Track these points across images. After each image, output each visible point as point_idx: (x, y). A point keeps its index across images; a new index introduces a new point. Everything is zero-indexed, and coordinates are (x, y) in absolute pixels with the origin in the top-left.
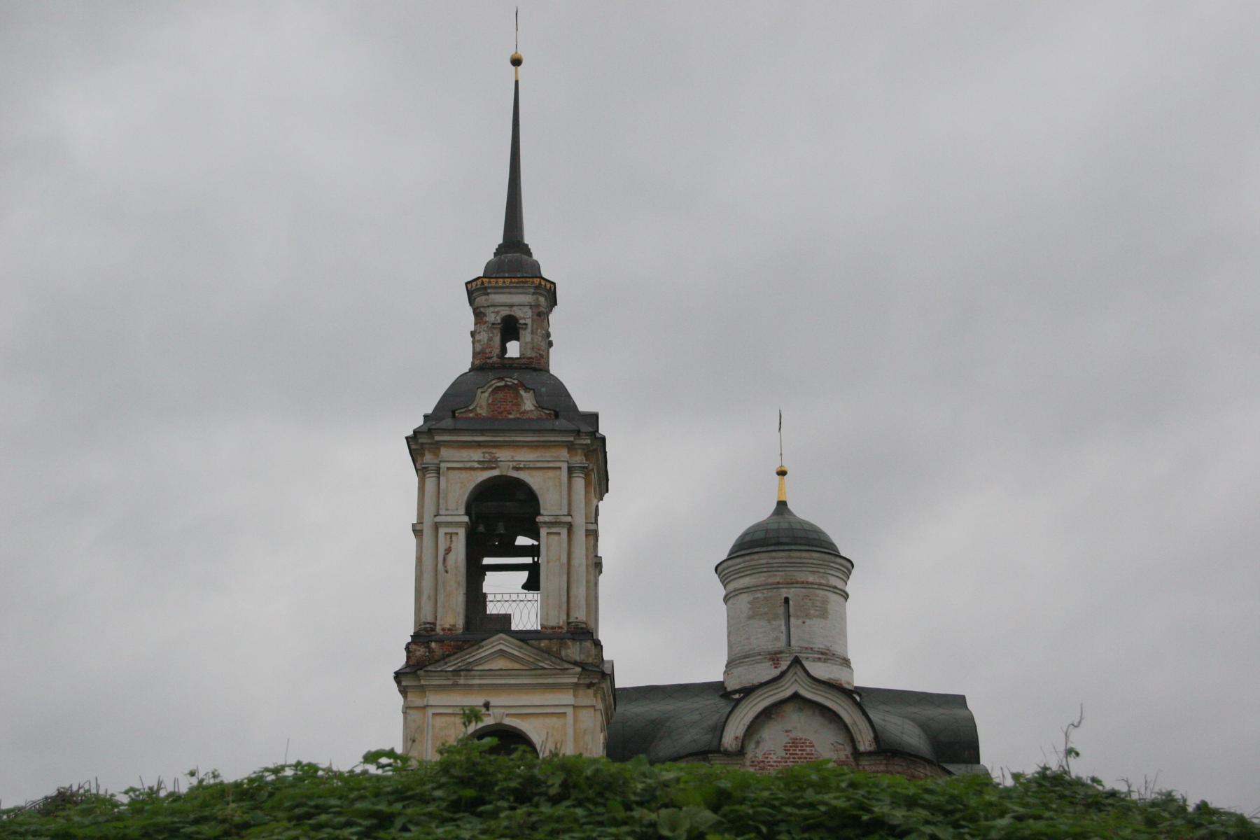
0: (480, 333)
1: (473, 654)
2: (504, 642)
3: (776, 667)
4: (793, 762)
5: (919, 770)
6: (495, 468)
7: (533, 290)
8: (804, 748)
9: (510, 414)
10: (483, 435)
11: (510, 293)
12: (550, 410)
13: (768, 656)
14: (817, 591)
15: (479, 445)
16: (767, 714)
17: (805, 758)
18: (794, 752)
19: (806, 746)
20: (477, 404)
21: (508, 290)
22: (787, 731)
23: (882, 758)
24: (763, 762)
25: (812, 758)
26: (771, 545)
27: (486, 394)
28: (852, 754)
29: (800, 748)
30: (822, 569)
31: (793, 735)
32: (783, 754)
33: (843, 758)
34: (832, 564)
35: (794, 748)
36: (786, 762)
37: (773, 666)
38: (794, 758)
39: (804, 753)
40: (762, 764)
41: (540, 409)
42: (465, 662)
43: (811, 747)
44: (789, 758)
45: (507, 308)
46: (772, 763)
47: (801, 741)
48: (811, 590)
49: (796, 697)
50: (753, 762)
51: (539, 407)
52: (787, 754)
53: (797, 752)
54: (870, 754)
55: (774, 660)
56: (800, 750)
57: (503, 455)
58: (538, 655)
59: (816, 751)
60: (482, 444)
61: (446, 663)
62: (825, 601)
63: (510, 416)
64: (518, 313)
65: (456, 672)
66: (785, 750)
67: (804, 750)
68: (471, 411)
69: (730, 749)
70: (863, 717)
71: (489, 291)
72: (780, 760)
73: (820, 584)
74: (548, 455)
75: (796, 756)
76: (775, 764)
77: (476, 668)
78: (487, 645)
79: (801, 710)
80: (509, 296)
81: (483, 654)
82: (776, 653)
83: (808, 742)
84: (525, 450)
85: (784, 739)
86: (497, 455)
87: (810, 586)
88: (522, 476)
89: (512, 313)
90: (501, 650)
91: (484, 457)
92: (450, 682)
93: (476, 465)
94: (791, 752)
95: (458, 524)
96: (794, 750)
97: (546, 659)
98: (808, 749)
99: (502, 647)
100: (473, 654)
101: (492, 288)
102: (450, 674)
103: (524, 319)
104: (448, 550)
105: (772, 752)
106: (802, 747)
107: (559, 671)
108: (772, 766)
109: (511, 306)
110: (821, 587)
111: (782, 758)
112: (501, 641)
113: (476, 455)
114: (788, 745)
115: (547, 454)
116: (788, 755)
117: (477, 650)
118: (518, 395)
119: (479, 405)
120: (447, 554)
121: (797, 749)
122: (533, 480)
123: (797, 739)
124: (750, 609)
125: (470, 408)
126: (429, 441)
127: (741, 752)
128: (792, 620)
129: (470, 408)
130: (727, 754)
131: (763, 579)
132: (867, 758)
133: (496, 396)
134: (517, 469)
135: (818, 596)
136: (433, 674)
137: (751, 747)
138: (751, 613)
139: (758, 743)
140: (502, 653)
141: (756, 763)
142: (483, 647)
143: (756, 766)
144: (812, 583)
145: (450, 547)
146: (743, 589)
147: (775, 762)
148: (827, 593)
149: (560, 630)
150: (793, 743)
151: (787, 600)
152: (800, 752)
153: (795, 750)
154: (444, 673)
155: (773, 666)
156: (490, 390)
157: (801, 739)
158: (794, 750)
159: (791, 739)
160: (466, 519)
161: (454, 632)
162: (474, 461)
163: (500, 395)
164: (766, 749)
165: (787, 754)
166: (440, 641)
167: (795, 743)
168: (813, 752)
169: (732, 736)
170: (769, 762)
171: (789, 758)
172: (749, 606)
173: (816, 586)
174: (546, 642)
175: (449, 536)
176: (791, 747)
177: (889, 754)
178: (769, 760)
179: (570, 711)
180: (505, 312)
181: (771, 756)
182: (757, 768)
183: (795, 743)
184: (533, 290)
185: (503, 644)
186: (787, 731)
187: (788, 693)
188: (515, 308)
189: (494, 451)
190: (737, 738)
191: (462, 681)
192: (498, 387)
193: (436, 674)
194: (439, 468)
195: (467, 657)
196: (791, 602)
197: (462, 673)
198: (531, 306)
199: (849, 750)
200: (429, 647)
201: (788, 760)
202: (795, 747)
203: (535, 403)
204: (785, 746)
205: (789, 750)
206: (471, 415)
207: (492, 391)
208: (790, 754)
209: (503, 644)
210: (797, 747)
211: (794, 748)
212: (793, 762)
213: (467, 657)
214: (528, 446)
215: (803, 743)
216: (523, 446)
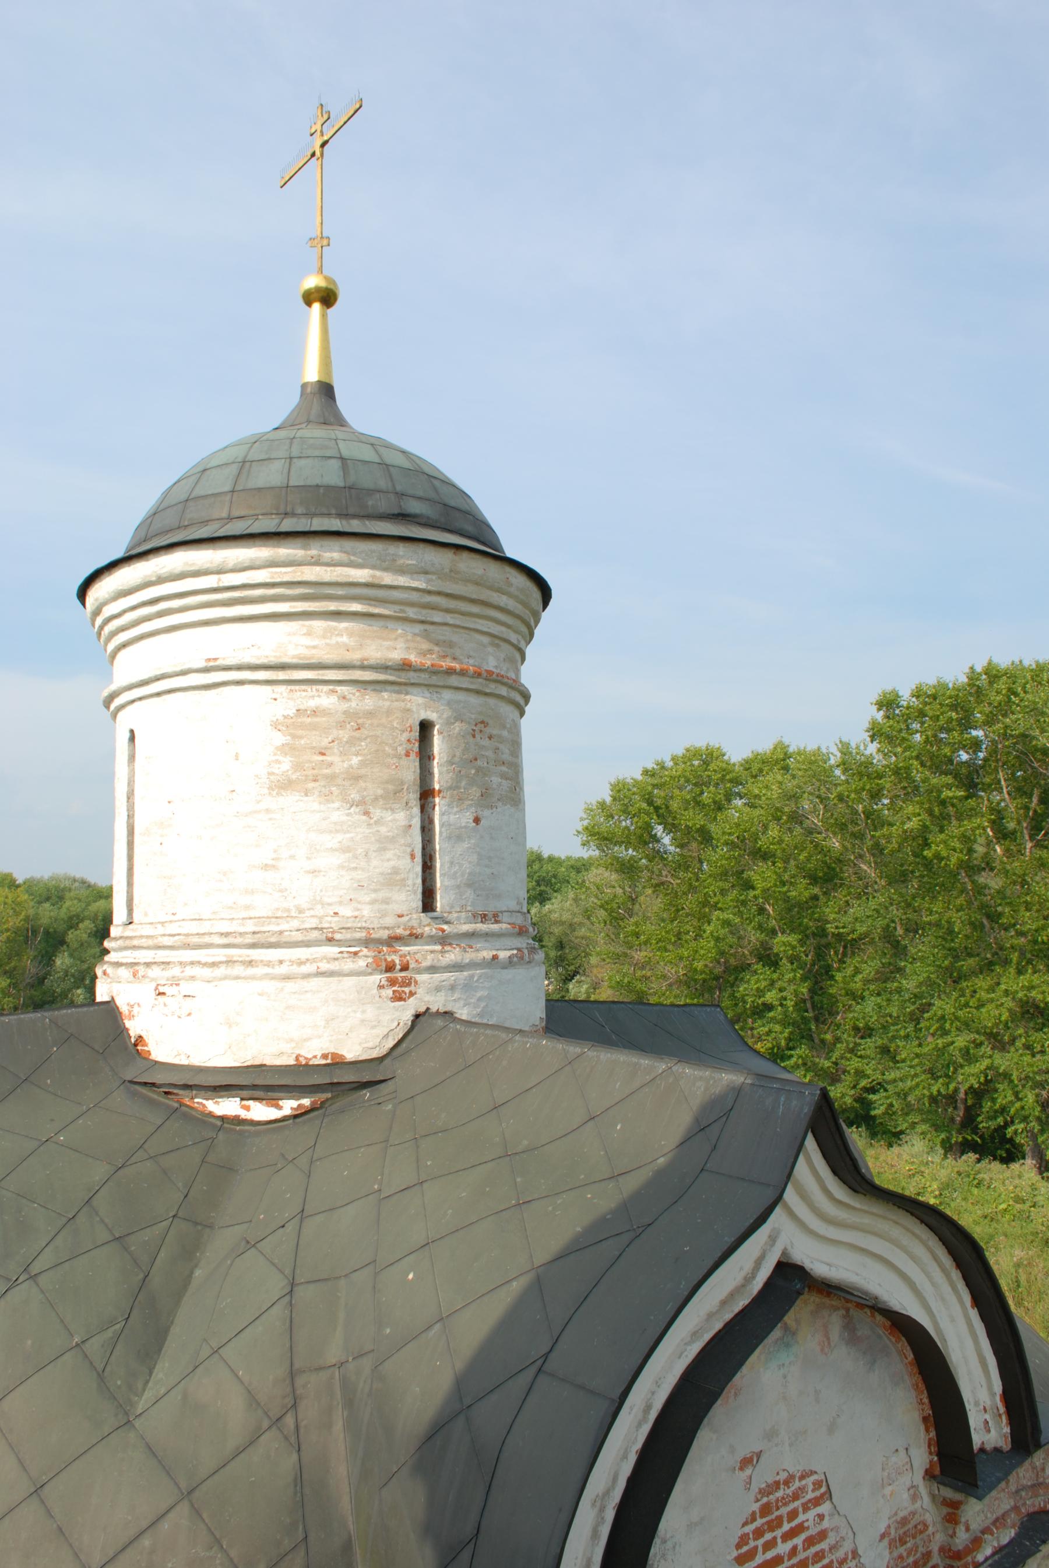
3: (398, 998)
31: (763, 1475)
37: (389, 992)
48: (492, 701)
55: (390, 968)
82: (394, 940)
83: (809, 1481)
124: (285, 749)
131: (345, 639)
135: (504, 727)
138: (286, 764)
146: (239, 668)
150: (765, 1510)
151: (425, 728)
168: (826, 1524)
172: (280, 739)
196: (438, 744)
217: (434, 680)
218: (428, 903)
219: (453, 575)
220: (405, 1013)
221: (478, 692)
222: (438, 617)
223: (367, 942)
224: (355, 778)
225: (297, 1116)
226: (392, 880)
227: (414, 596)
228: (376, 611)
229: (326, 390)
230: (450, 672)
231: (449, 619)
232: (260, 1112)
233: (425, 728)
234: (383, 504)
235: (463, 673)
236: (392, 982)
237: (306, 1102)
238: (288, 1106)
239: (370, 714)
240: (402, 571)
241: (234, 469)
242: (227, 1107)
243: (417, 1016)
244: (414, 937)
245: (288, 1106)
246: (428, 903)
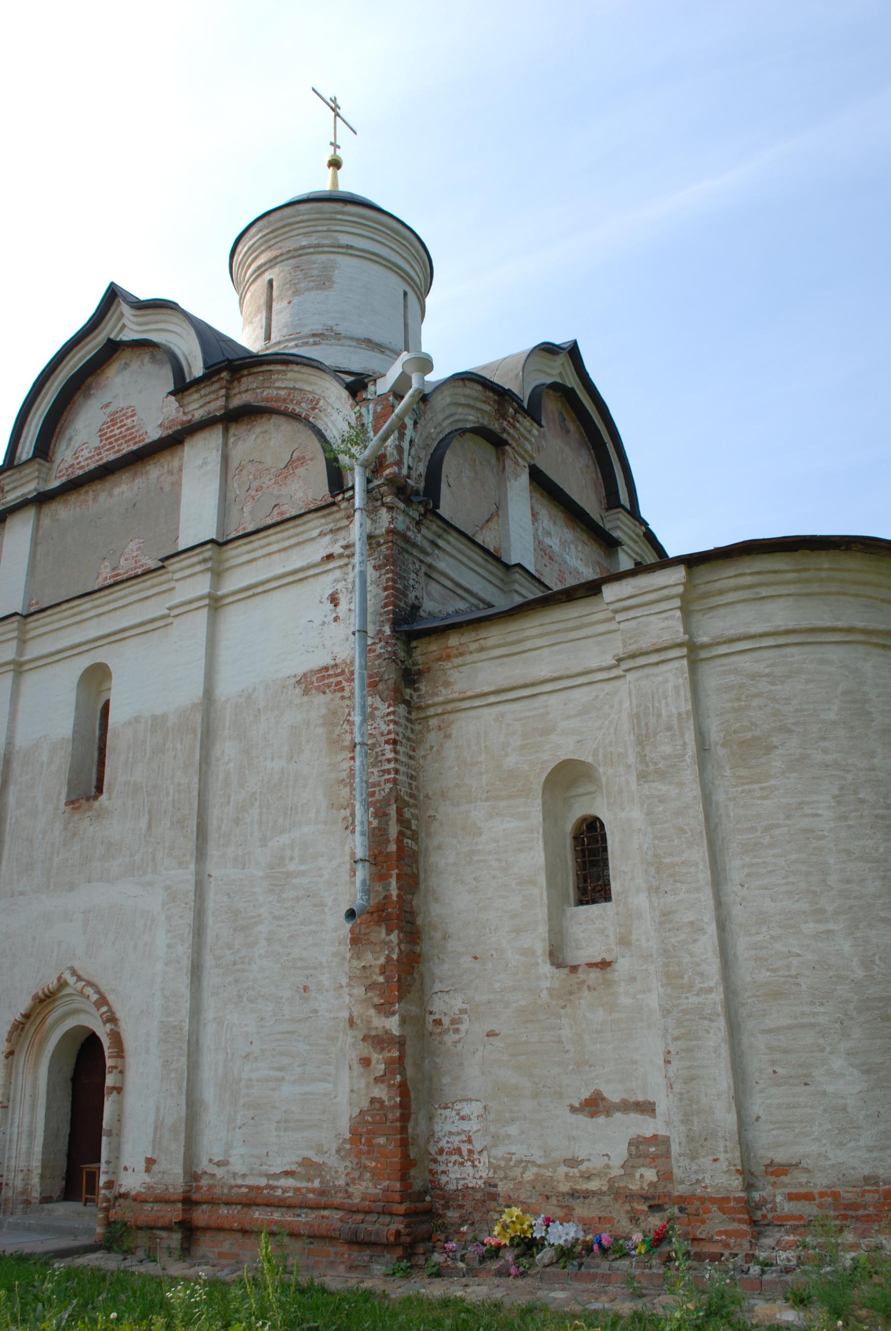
5: (278, 384)
14: (314, 257)
30: (323, 225)
34: (339, 217)
38: (110, 443)
44: (103, 446)
48: (304, 258)
52: (101, 441)
87: (301, 252)
96: (111, 431)
148: (332, 257)
150: (112, 420)
168: (135, 423)
196: (275, 284)
217: (272, 263)
221: (294, 257)
222: (272, 242)
227: (261, 241)
230: (276, 258)
231: (277, 240)
235: (281, 255)
240: (254, 236)
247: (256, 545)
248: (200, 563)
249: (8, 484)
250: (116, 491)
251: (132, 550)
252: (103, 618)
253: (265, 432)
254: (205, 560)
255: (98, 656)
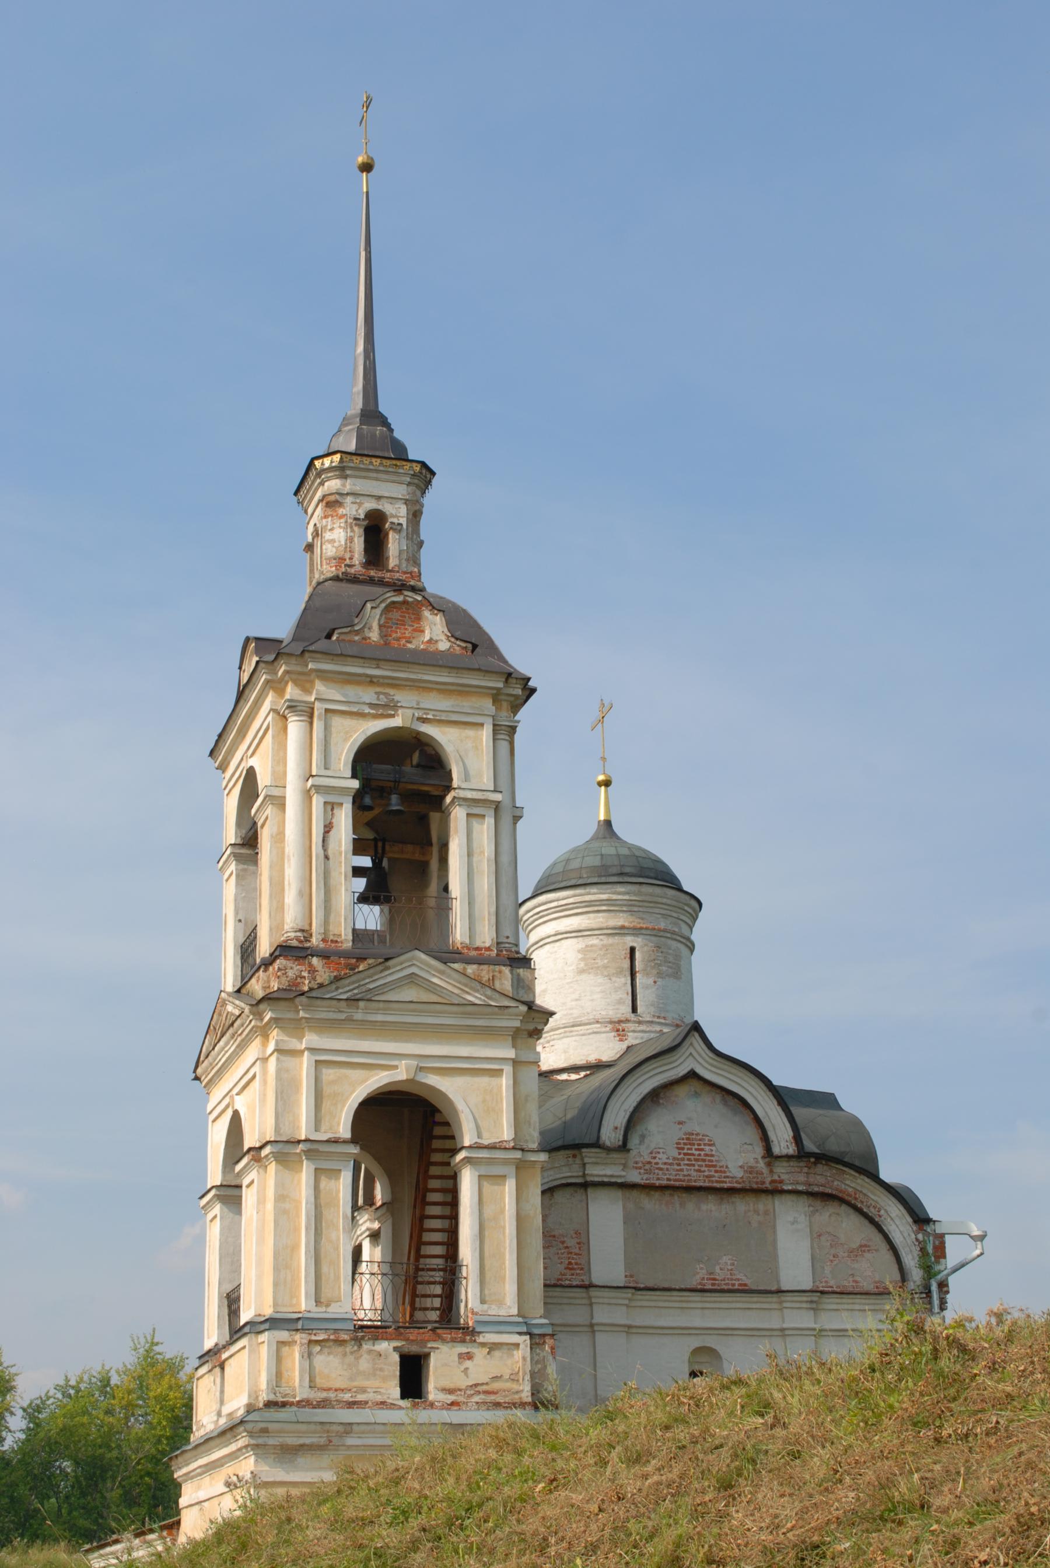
0: (332, 530)
1: (376, 977)
2: (418, 964)
3: (621, 1040)
4: (687, 1165)
5: (847, 1182)
6: (393, 716)
7: (408, 479)
8: (702, 1147)
9: (410, 642)
10: (378, 667)
11: (377, 479)
12: (466, 642)
13: (610, 1026)
14: (670, 942)
15: (371, 681)
16: (654, 1096)
17: (704, 1160)
18: (689, 1152)
19: (705, 1145)
20: (366, 624)
21: (375, 475)
22: (680, 1123)
23: (802, 1164)
24: (649, 1163)
25: (712, 1161)
26: (614, 875)
27: (378, 611)
28: (763, 1157)
29: (696, 1147)
30: (676, 912)
31: (687, 1128)
32: (675, 1153)
33: (752, 1163)
35: (689, 1146)
36: (679, 1165)
37: (618, 1038)
38: (689, 1160)
39: (702, 1153)
40: (647, 1167)
41: (453, 640)
42: (364, 989)
43: (710, 1145)
44: (683, 1159)
45: (373, 500)
46: (661, 1166)
47: (698, 1138)
48: (663, 939)
49: (692, 1075)
50: (636, 1163)
51: (452, 636)
52: (680, 1154)
53: (694, 1152)
54: (788, 1157)
55: (618, 1030)
56: (696, 1150)
57: (403, 697)
58: (466, 985)
59: (717, 1151)
60: (375, 680)
61: (337, 989)
62: (678, 957)
63: (409, 646)
64: (387, 508)
65: (353, 1001)
66: (678, 1148)
67: (702, 1150)
68: (357, 632)
69: (608, 1143)
70: (779, 1109)
71: (348, 472)
72: (671, 1161)
73: (674, 933)
74: (467, 704)
75: (692, 1157)
76: (665, 1167)
77: (376, 998)
78: (395, 966)
79: (697, 1094)
80: (375, 483)
81: (389, 979)
82: (620, 1022)
84: (433, 694)
85: (676, 1134)
86: (396, 698)
87: (662, 934)
88: (425, 729)
89: (380, 507)
90: (413, 973)
91: (378, 699)
92: (343, 1016)
93: (367, 710)
94: (685, 1151)
95: (342, 791)
96: (688, 1149)
97: (477, 991)
98: (707, 1148)
99: (413, 970)
100: (376, 977)
101: (351, 468)
102: (343, 1004)
103: (397, 517)
104: (328, 828)
105: (661, 1151)
106: (699, 1145)
107: (497, 1009)
108: (661, 1169)
109: (379, 498)
110: (675, 937)
111: (674, 1159)
112: (415, 962)
113: (368, 695)
114: (682, 1141)
115: (465, 704)
116: (682, 1156)
117: (382, 971)
118: (419, 618)
119: (367, 626)
120: (328, 832)
121: (694, 1147)
122: (445, 738)
123: (693, 1134)
124: (582, 959)
125: (357, 628)
126: (299, 669)
127: (624, 1147)
128: (639, 977)
129: (357, 628)
130: (609, 1150)
131: (601, 920)
132: (785, 1164)
133: (390, 615)
134: (424, 720)
135: (670, 949)
136: (319, 1002)
137: (634, 1142)
138: (582, 965)
139: (643, 1137)
140: (412, 979)
141: (640, 1165)
142: (388, 968)
143: (640, 1168)
144: (665, 931)
145: (331, 823)
146: (566, 933)
147: (665, 1164)
148: (679, 945)
149: (488, 953)
150: (688, 1139)
151: (632, 950)
152: (697, 1153)
153: (691, 1149)
154: (334, 1002)
155: (618, 1038)
156: (383, 605)
157: (697, 1134)
158: (688, 1149)
159: (686, 1134)
160: (355, 784)
161: (340, 945)
162: (364, 703)
163: (396, 615)
164: (653, 1146)
165: (680, 1154)
166: (324, 955)
167: (690, 1139)
168: (713, 1153)
169: (611, 1127)
170: (657, 1163)
171: (683, 1159)
172: (580, 956)
173: (669, 935)
174: (475, 967)
175: (329, 808)
176: (685, 1144)
177: (812, 1160)
178: (657, 1160)
179: (508, 1069)
180: (370, 505)
181: (658, 1156)
182: (642, 1171)
183: (690, 1139)
184: (408, 479)
185: (418, 966)
186: (680, 1123)
187: (682, 1071)
188: (383, 501)
189: (391, 691)
190: (616, 1128)
191: (359, 1016)
192: (393, 603)
193: (325, 1003)
194: (313, 709)
195: (367, 981)
196: (638, 955)
197: (361, 1004)
198: (406, 502)
199: (759, 1150)
200: (310, 965)
201: (682, 1163)
202: (690, 1144)
203: (446, 630)
204: (677, 1144)
205: (683, 1149)
206: (356, 638)
207: (386, 607)
208: (685, 1154)
209: (418, 966)
210: (694, 1145)
211: (689, 1146)
212: (687, 1165)
213: (367, 981)
214: (440, 691)
215: (700, 1140)
216: (431, 690)
217: (635, 932)
218: (634, 1010)
219: (640, 893)
220: (624, 1046)
221: (655, 936)
222: (636, 909)
223: (611, 1022)
224: (605, 967)
225: (586, 1076)
226: (620, 1002)
227: (625, 902)
228: (612, 908)
229: (608, 823)
230: (641, 928)
231: (641, 909)
232: (574, 1077)
233: (632, 950)
234: (614, 870)
235: (647, 928)
236: (619, 1035)
237: (588, 1072)
238: (582, 1074)
239: (611, 945)
240: (619, 893)
241: (564, 863)
242: (564, 1077)
243: (628, 1047)
244: (627, 1021)
245: (582, 1074)
246: (634, 1010)
247: (844, 1301)
248: (807, 1302)
249: (590, 1157)
250: (704, 1207)
251: (726, 1263)
252: (706, 1311)
253: (838, 1214)
254: (812, 1302)
255: (710, 1342)
